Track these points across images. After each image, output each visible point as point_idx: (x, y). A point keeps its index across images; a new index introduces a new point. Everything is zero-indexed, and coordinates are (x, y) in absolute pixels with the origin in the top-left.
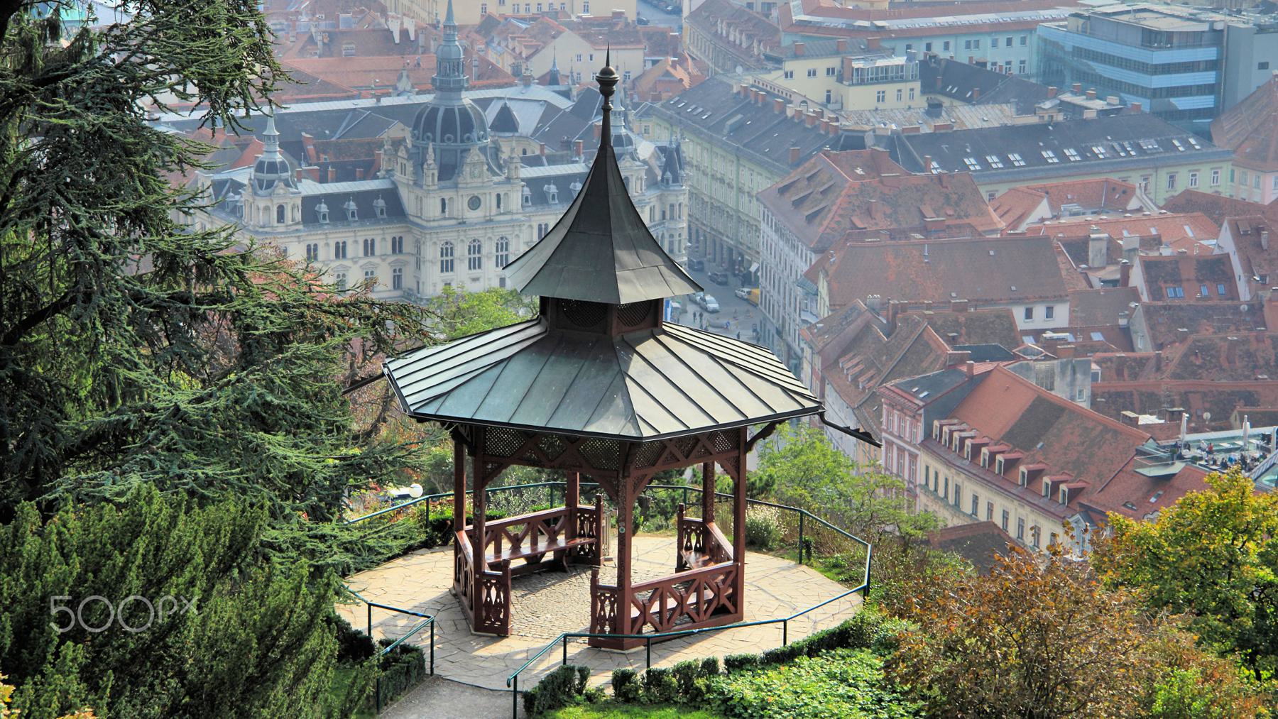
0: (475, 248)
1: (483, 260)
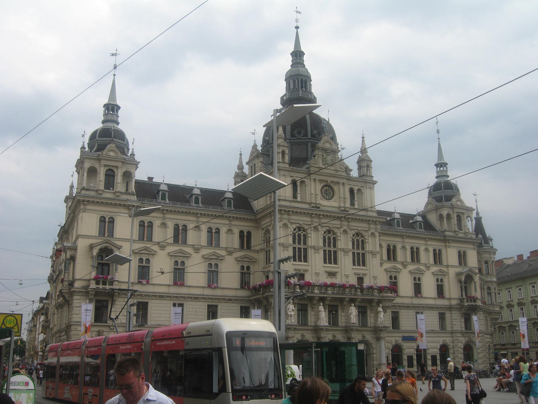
0: (330, 239)
1: (340, 255)
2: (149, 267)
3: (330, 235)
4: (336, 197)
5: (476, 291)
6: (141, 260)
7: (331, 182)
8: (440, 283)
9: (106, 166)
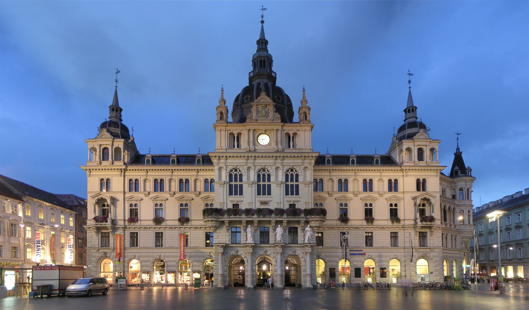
1: (273, 187)
8: (394, 207)
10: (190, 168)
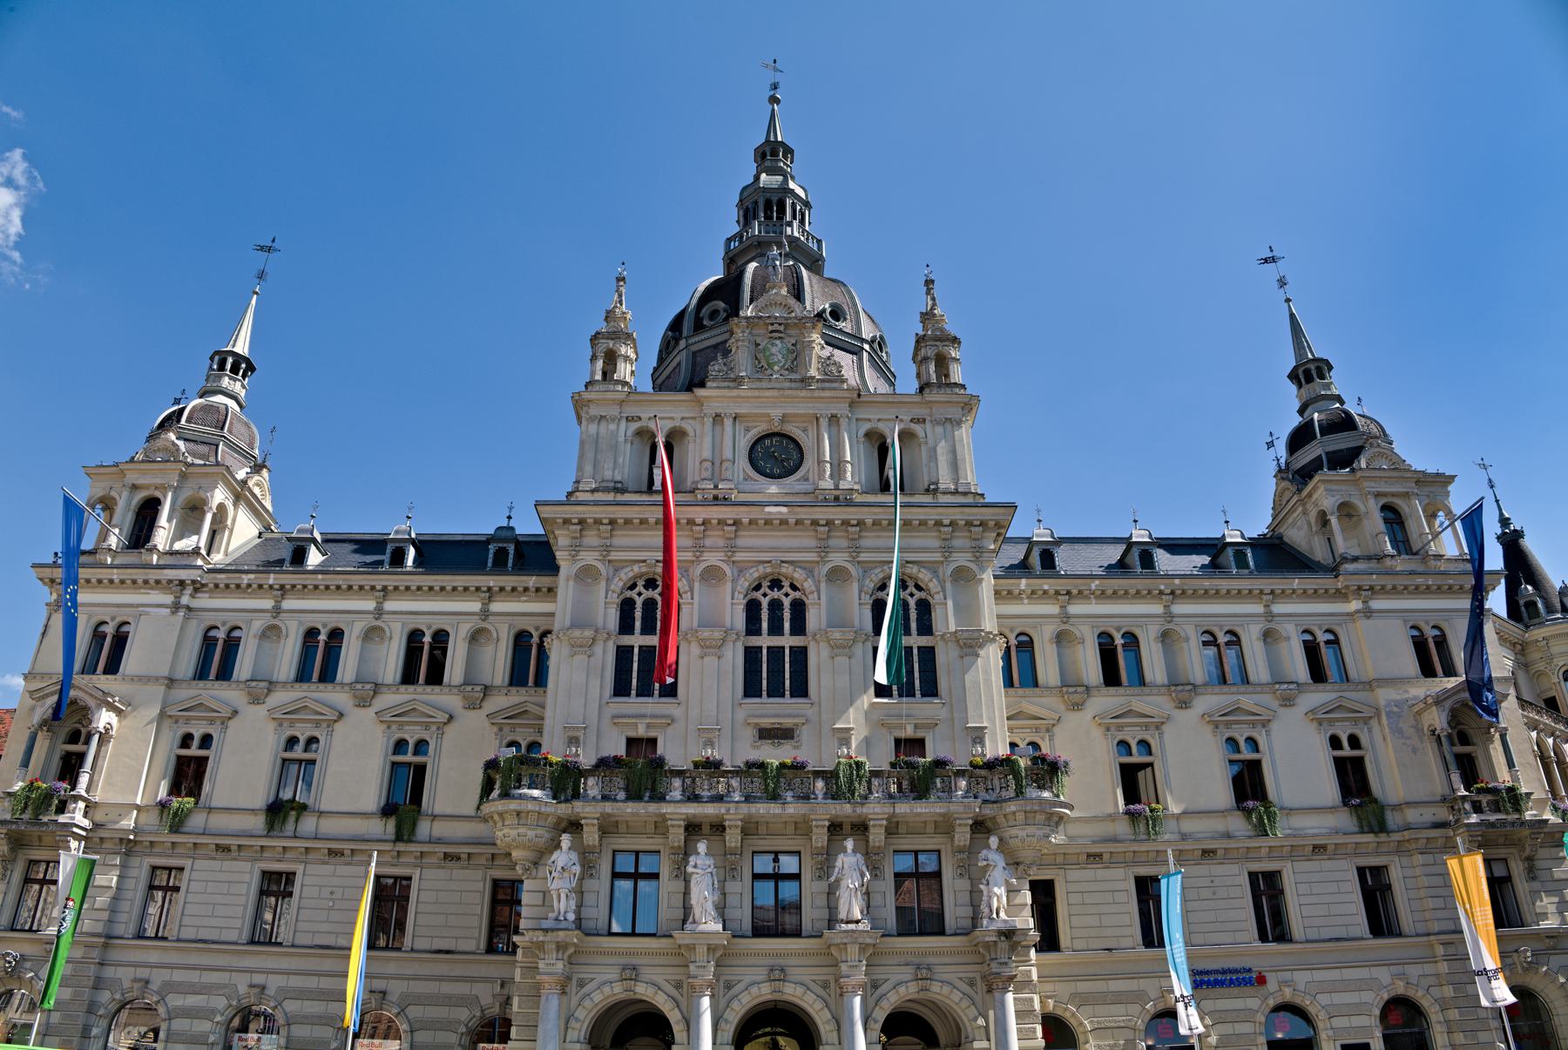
2: (207, 758)
3: (776, 594)
4: (809, 463)
5: (1511, 764)
6: (186, 740)
7: (784, 419)
8: (1347, 751)
9: (135, 487)
10: (460, 580)
